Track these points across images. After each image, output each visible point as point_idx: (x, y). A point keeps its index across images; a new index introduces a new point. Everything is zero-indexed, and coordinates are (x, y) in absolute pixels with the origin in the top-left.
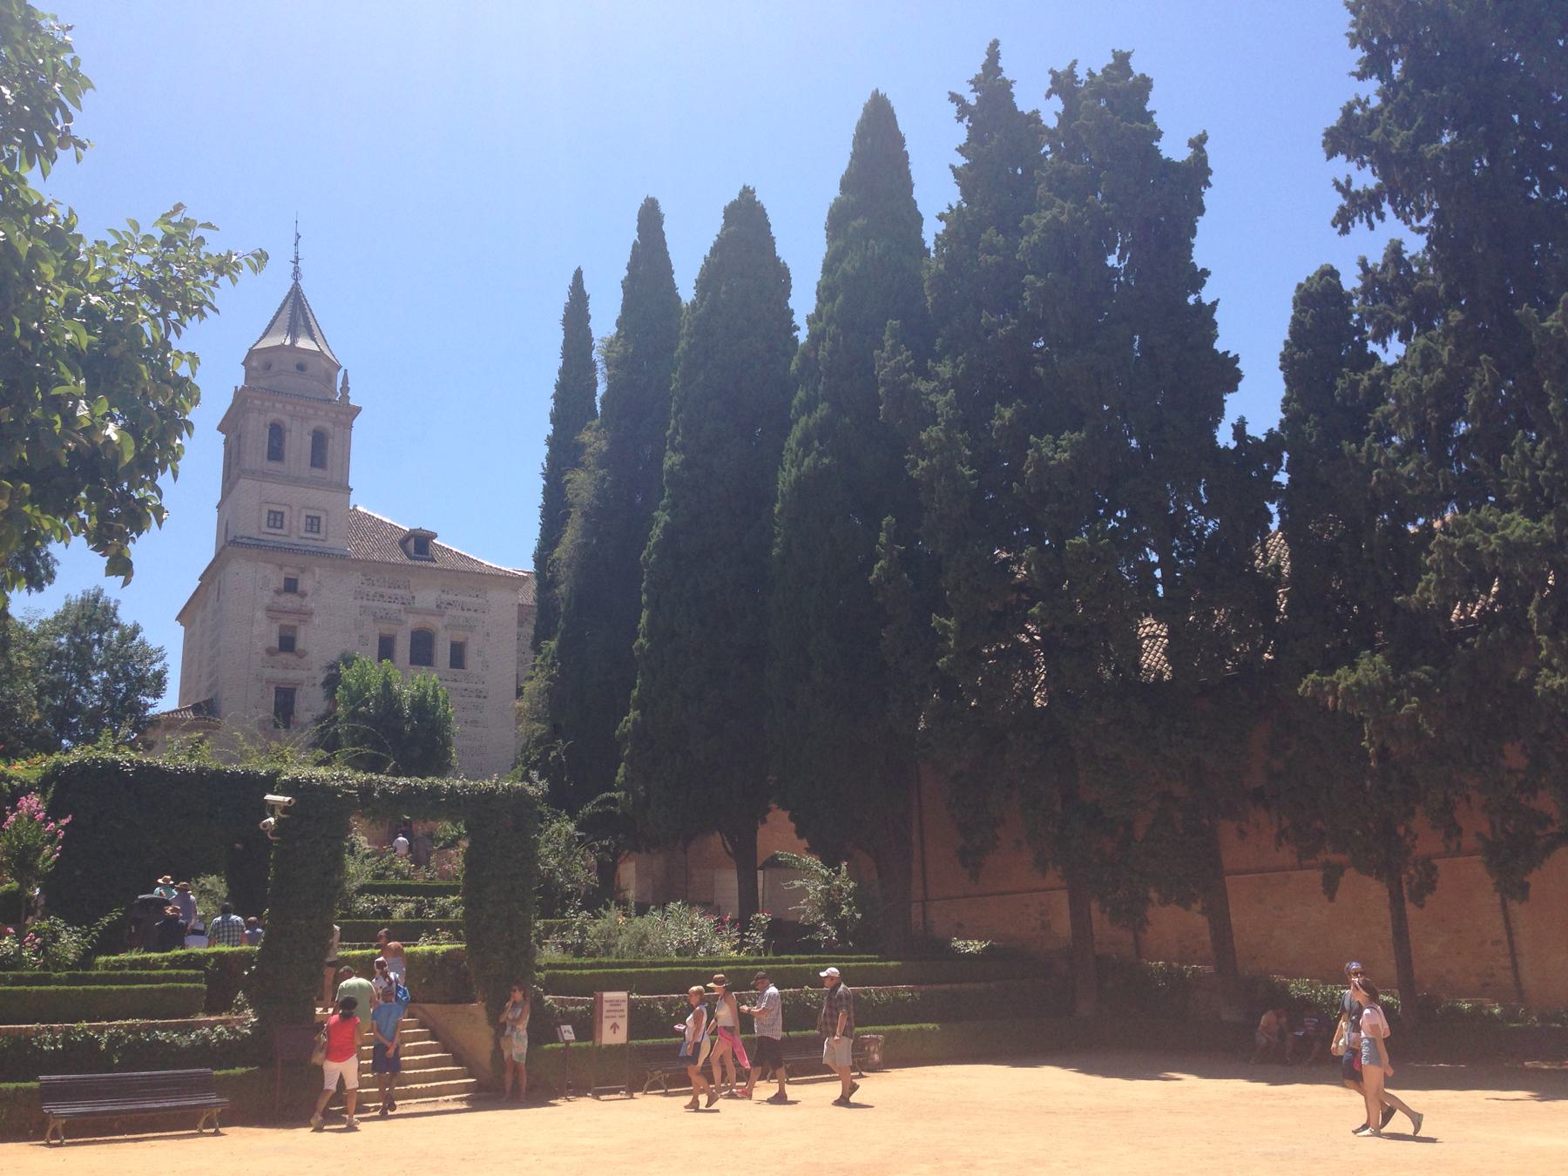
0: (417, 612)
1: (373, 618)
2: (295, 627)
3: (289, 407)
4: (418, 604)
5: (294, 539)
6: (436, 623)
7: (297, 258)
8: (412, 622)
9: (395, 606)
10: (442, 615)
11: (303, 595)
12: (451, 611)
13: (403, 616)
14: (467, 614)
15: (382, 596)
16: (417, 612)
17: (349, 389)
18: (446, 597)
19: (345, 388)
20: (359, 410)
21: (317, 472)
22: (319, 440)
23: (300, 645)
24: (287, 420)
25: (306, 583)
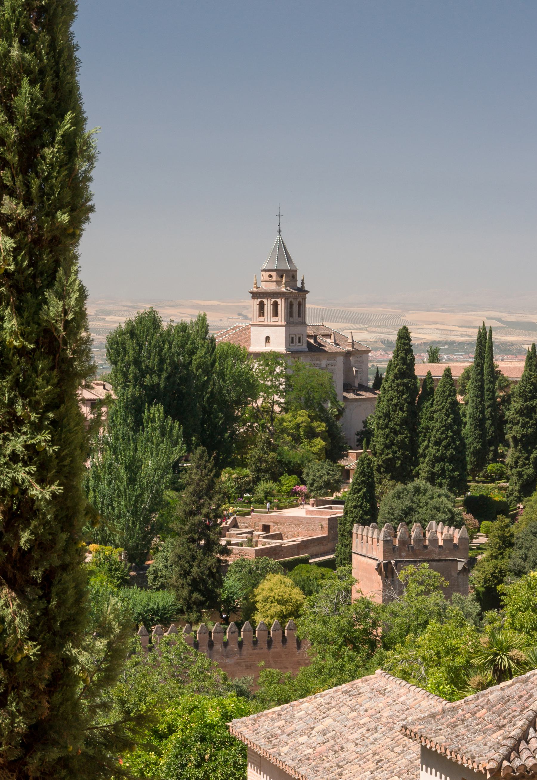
5: (296, 347)
9: (318, 368)
14: (333, 367)
18: (328, 362)
19: (303, 283)
20: (308, 292)
21: (300, 319)
22: (300, 305)
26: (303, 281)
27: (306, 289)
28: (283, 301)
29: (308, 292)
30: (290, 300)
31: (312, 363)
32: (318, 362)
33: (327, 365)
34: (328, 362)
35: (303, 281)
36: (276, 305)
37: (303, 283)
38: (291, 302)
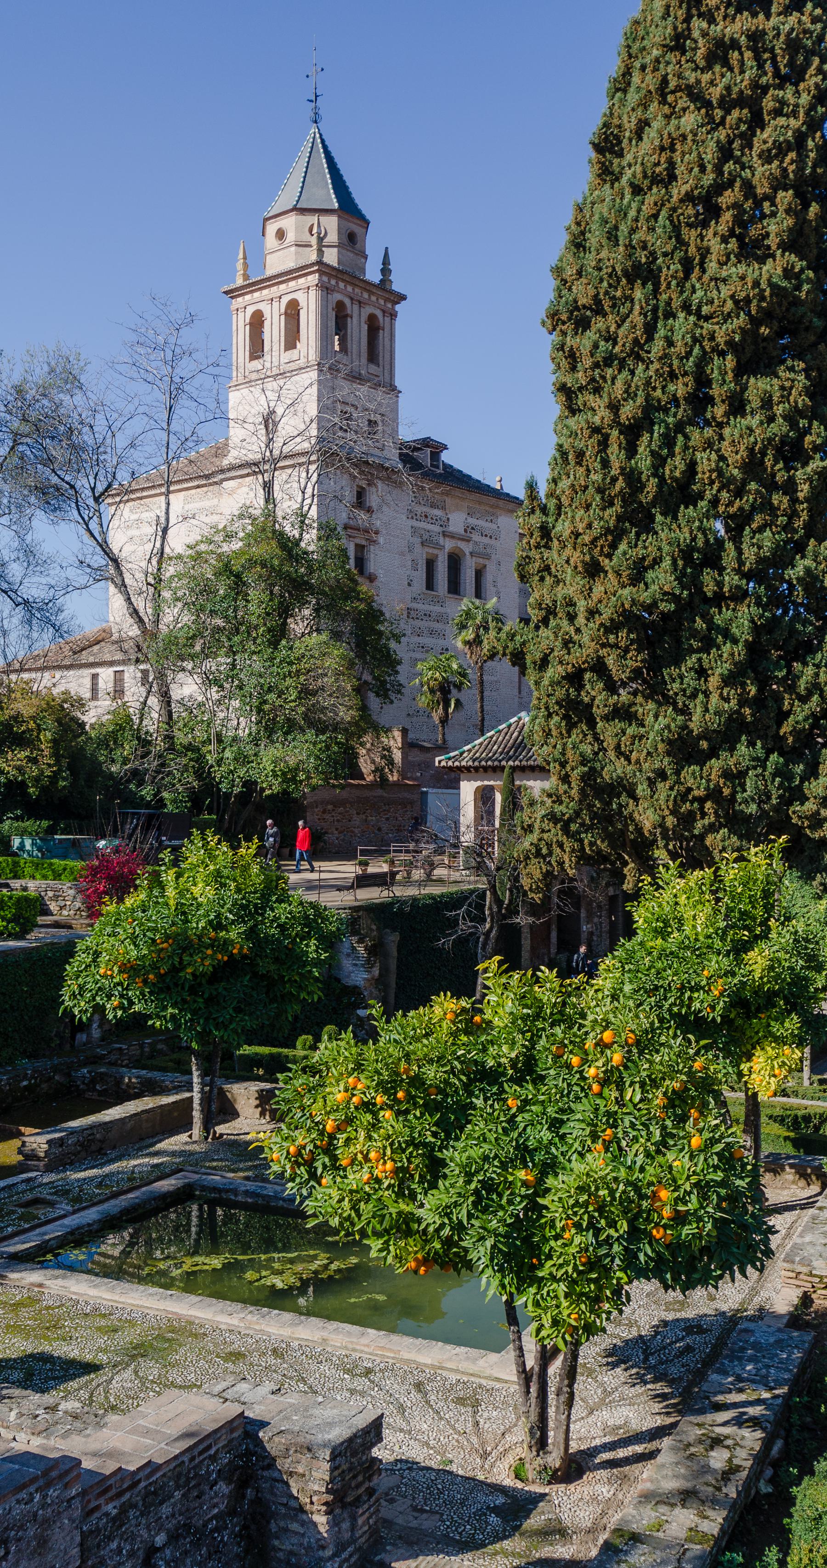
0: (452, 536)
1: (420, 540)
2: (363, 547)
3: (350, 289)
4: (451, 528)
6: (466, 548)
7: (316, 96)
8: (449, 545)
9: (436, 528)
10: (468, 541)
11: (369, 510)
12: (476, 537)
13: (441, 540)
14: (486, 540)
15: (426, 516)
16: (452, 536)
17: (390, 271)
18: (472, 521)
19: (386, 270)
20: (403, 298)
21: (373, 368)
23: (372, 567)
24: (347, 301)
25: (373, 499)
26: (386, 261)
27: (395, 287)
28: (313, 293)
29: (403, 298)
30: (338, 297)
31: (420, 509)
32: (437, 512)
33: (469, 529)
34: (472, 521)
35: (386, 261)
36: (293, 312)
37: (386, 270)
38: (340, 306)
